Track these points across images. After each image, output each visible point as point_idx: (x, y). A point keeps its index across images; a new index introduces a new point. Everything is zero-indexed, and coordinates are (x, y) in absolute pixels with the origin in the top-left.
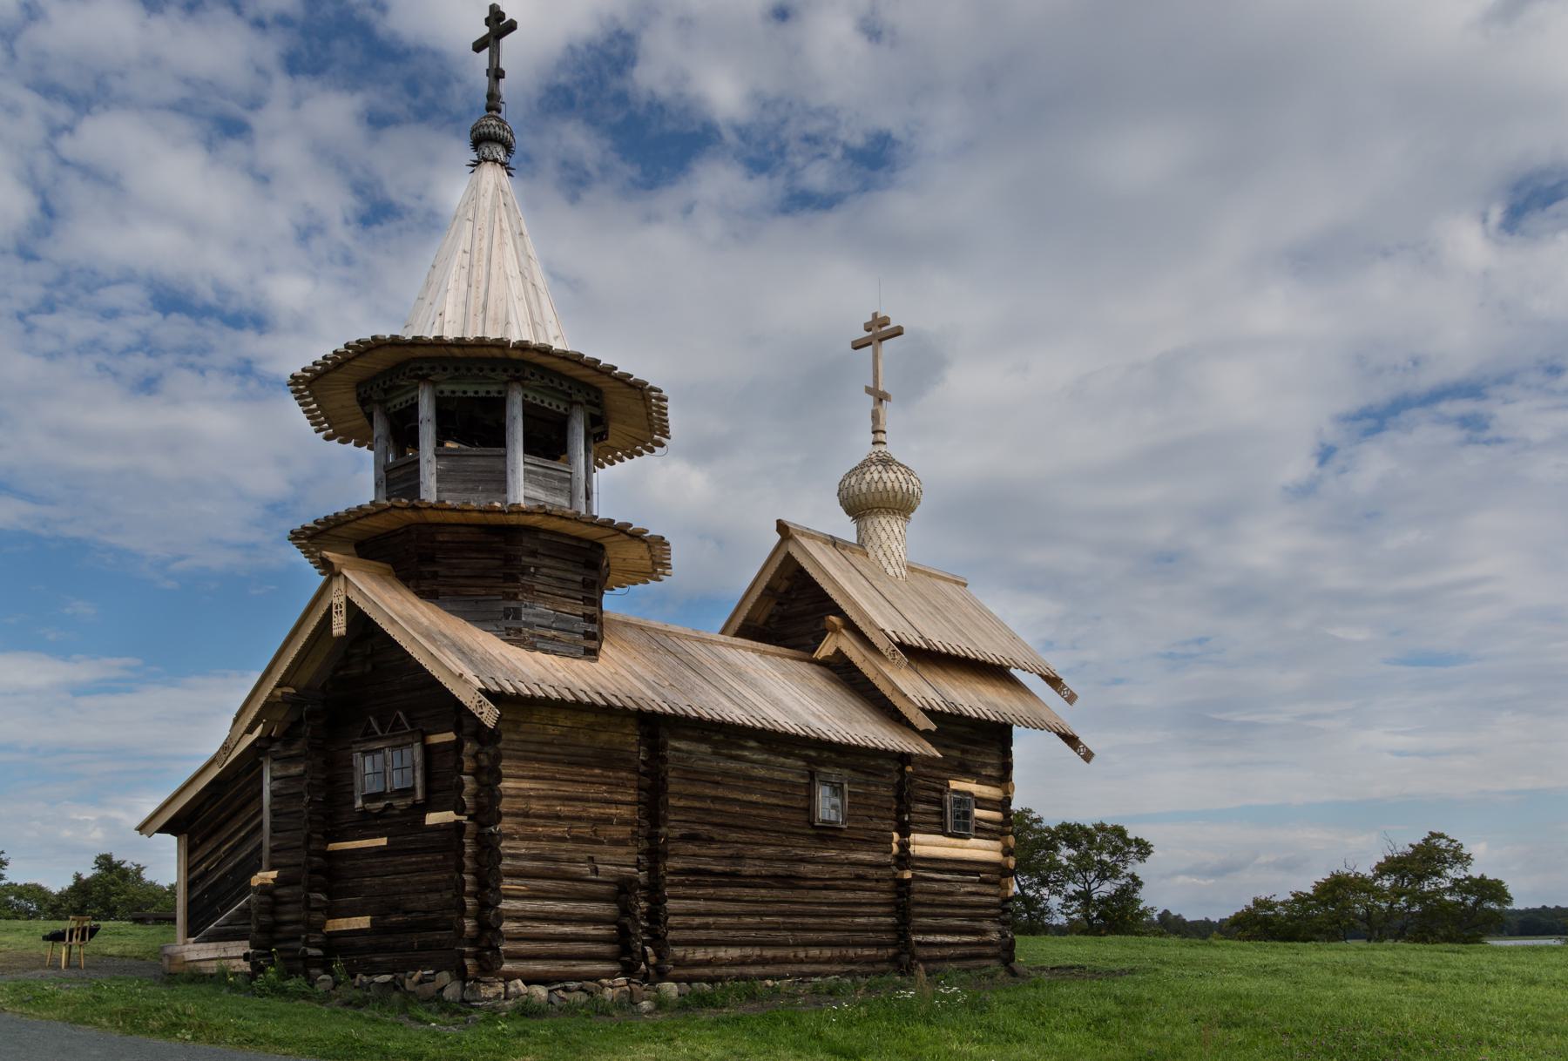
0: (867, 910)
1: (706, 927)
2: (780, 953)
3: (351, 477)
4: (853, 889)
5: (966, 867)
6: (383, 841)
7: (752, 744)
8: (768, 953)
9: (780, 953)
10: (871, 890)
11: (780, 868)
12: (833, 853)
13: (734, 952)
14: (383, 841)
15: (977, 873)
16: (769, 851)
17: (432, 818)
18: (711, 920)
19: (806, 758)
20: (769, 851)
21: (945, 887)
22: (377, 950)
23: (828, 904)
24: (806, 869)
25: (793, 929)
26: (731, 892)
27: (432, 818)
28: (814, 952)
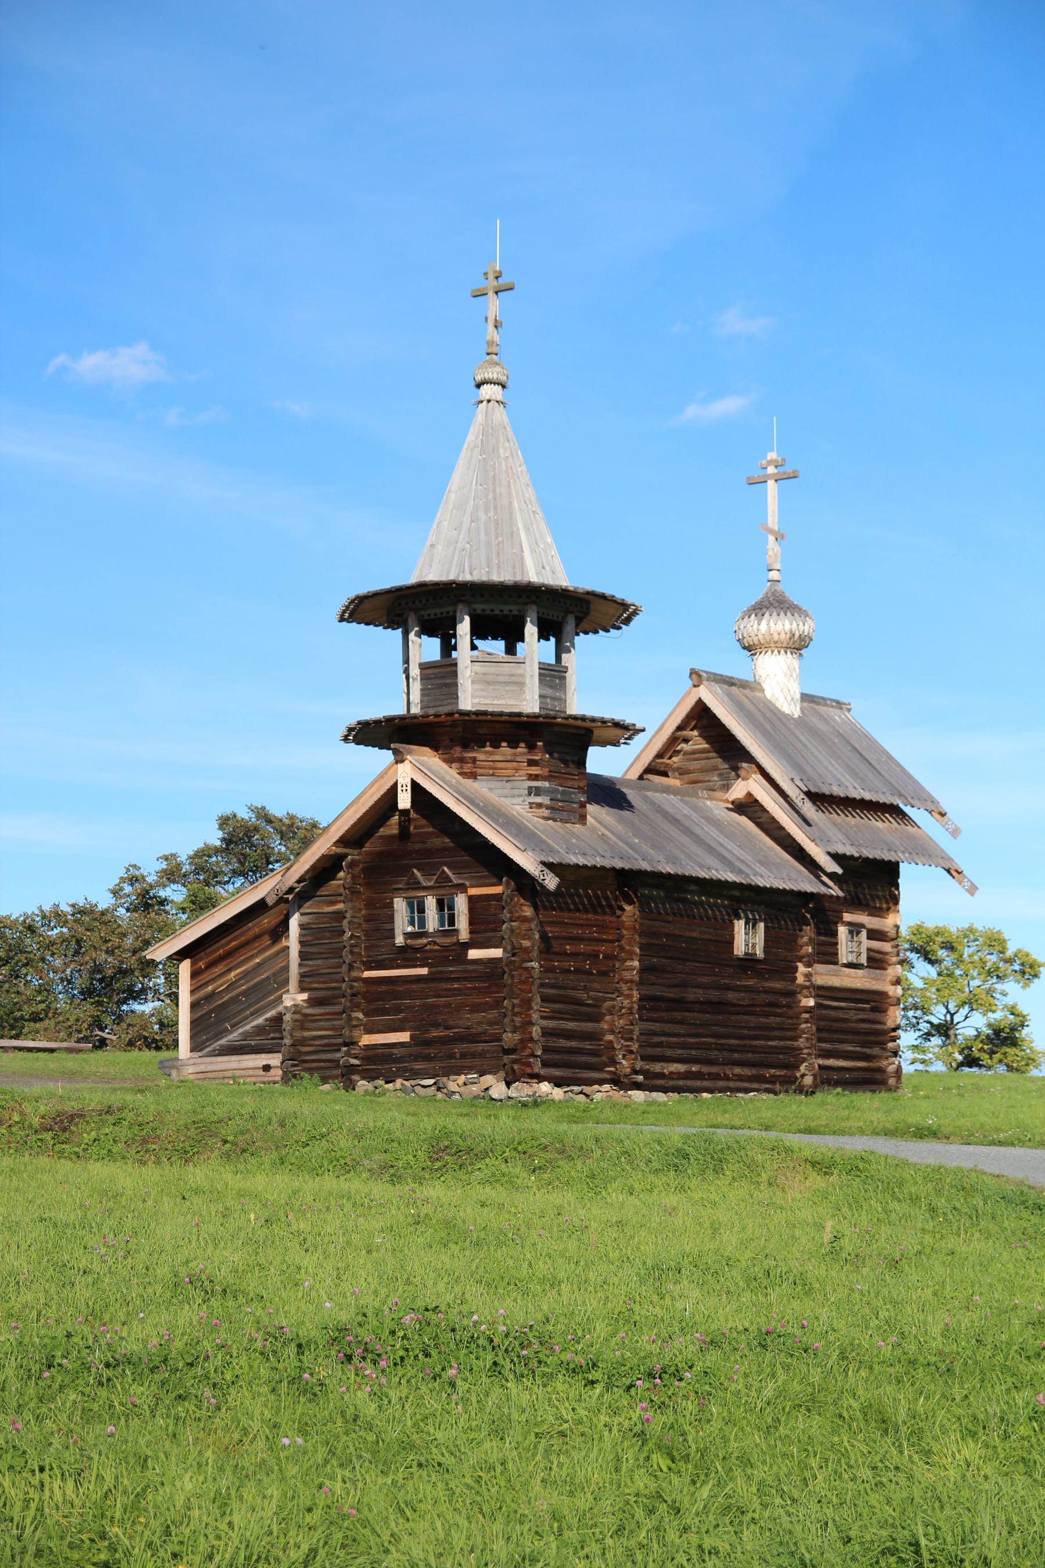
0: (777, 1033)
1: (659, 1045)
2: (714, 1069)
3: (385, 674)
4: (767, 1015)
5: (859, 996)
6: (424, 971)
7: (693, 887)
8: (705, 1069)
9: (714, 1069)
10: (780, 1015)
11: (714, 995)
12: (751, 983)
13: (680, 1068)
14: (424, 971)
15: (867, 1002)
16: (705, 980)
17: (474, 954)
18: (664, 1039)
19: (731, 898)
20: (705, 980)
21: (841, 1014)
22: (417, 1058)
23: (749, 1028)
24: (731, 996)
25: (721, 1048)
26: (678, 1015)
27: (474, 954)
28: (737, 1070)
